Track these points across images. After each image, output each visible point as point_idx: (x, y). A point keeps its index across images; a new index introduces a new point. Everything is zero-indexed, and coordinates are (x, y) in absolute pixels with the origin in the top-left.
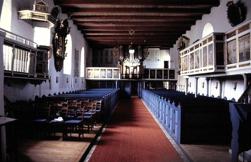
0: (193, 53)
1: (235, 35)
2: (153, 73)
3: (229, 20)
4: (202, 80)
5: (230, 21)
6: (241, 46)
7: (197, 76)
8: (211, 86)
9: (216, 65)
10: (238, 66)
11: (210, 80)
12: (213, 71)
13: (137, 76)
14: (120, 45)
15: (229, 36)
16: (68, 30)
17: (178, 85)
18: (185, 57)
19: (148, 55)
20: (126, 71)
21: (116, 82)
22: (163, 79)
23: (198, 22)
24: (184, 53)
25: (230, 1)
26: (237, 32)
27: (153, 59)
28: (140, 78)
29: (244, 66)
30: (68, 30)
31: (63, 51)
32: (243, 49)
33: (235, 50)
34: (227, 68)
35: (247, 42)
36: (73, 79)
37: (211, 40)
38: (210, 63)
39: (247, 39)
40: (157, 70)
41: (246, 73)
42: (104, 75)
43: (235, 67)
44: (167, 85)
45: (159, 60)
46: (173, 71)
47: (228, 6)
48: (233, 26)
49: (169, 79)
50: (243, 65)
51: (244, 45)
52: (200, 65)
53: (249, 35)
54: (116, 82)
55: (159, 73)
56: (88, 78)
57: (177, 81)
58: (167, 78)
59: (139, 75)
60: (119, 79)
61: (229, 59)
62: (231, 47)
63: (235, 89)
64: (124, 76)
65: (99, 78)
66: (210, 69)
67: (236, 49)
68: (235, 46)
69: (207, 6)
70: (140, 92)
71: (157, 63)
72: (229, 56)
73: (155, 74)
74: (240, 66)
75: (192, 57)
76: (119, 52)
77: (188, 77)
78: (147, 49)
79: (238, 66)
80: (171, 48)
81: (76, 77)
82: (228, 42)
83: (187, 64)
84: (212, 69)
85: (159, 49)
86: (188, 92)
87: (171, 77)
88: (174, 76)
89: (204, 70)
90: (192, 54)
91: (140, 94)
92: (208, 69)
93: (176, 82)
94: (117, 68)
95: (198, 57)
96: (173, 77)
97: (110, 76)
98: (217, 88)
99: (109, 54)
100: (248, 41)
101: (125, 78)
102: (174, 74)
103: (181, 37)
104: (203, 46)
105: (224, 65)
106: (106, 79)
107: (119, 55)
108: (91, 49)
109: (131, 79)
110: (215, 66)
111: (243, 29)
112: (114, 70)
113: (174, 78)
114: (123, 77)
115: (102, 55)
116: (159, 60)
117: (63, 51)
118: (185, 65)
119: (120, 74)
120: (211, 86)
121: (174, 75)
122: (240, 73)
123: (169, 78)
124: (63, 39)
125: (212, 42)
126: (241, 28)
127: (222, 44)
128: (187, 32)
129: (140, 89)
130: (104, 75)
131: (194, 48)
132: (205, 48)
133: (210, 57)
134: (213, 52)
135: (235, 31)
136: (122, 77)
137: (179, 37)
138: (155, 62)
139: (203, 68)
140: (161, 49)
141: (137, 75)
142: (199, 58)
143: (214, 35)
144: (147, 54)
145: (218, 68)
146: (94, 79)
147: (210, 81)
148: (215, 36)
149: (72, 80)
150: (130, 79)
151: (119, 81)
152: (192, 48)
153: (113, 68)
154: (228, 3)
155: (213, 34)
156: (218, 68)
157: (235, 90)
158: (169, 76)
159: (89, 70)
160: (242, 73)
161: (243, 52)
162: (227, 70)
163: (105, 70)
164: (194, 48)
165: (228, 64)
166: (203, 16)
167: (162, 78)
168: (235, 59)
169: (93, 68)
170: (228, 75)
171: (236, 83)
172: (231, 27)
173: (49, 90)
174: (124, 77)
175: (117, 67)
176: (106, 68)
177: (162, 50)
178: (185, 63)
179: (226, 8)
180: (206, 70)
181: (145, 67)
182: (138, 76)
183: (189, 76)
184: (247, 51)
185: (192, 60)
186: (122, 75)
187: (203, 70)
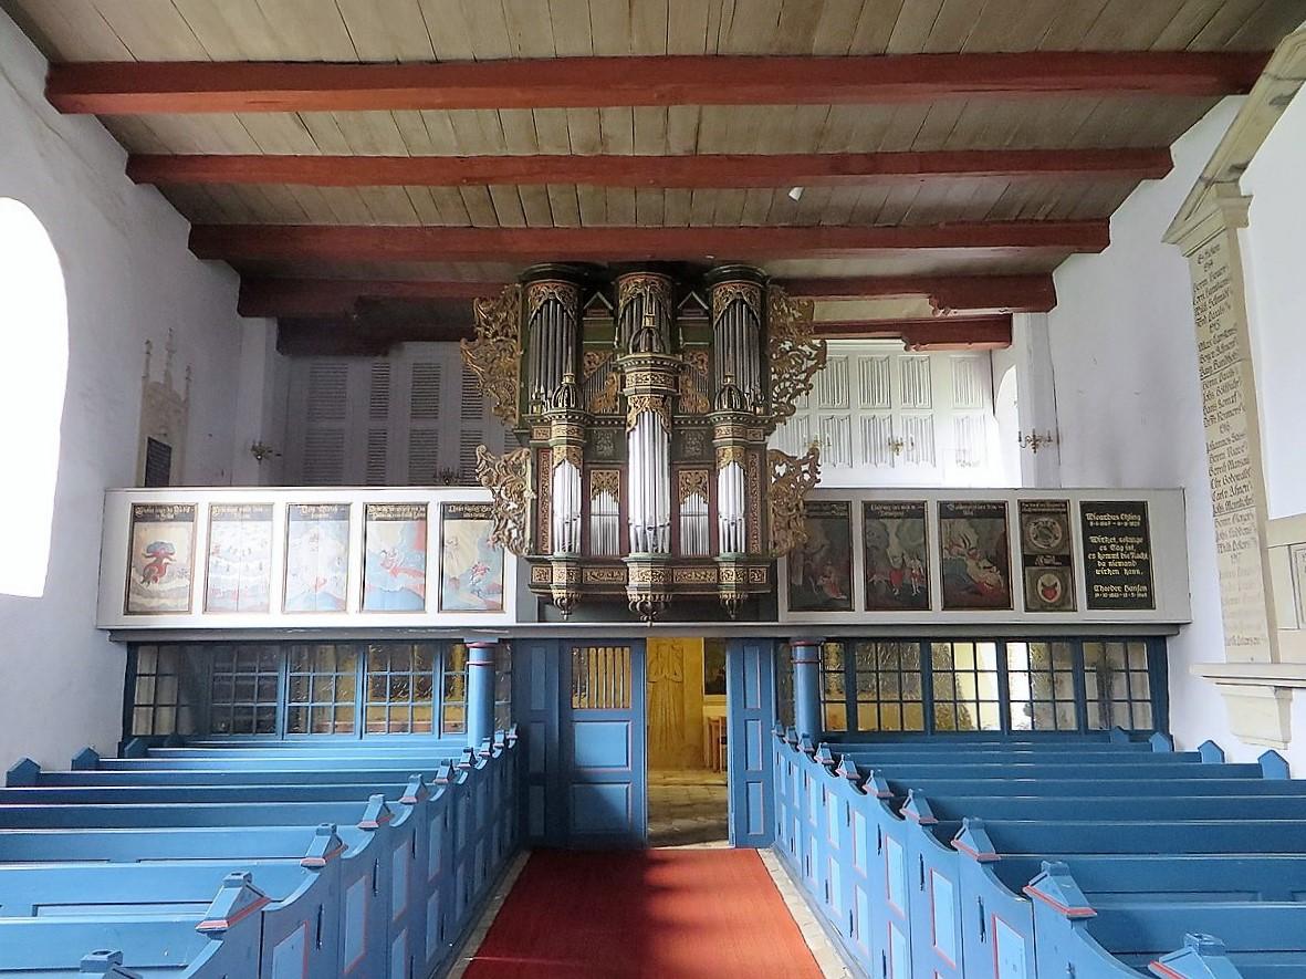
2: (894, 549)
13: (717, 586)
19: (810, 371)
21: (475, 656)
28: (757, 604)
40: (949, 511)
46: (1132, 520)
54: (475, 656)
55: (973, 538)
56: (128, 612)
58: (1066, 603)
60: (508, 618)
64: (560, 575)
65: (267, 610)
70: (756, 763)
73: (925, 561)
80: (1021, 321)
85: (899, 344)
87: (1106, 580)
88: (1146, 579)
91: (756, 791)
94: (482, 495)
96: (1136, 584)
97: (403, 581)
99: (450, 395)
101: (570, 606)
107: (524, 378)
113: (1148, 603)
115: (379, 403)
116: (896, 446)
119: (511, 560)
121: (1145, 566)
123: (1093, 604)
129: (755, 729)
138: (858, 458)
141: (710, 562)
146: (198, 620)
153: (434, 497)
158: (1091, 580)
159: (143, 514)
163: (343, 512)
167: (1006, 604)
174: (556, 594)
176: (357, 497)
181: (814, 470)
182: (730, 576)
186: (536, 574)
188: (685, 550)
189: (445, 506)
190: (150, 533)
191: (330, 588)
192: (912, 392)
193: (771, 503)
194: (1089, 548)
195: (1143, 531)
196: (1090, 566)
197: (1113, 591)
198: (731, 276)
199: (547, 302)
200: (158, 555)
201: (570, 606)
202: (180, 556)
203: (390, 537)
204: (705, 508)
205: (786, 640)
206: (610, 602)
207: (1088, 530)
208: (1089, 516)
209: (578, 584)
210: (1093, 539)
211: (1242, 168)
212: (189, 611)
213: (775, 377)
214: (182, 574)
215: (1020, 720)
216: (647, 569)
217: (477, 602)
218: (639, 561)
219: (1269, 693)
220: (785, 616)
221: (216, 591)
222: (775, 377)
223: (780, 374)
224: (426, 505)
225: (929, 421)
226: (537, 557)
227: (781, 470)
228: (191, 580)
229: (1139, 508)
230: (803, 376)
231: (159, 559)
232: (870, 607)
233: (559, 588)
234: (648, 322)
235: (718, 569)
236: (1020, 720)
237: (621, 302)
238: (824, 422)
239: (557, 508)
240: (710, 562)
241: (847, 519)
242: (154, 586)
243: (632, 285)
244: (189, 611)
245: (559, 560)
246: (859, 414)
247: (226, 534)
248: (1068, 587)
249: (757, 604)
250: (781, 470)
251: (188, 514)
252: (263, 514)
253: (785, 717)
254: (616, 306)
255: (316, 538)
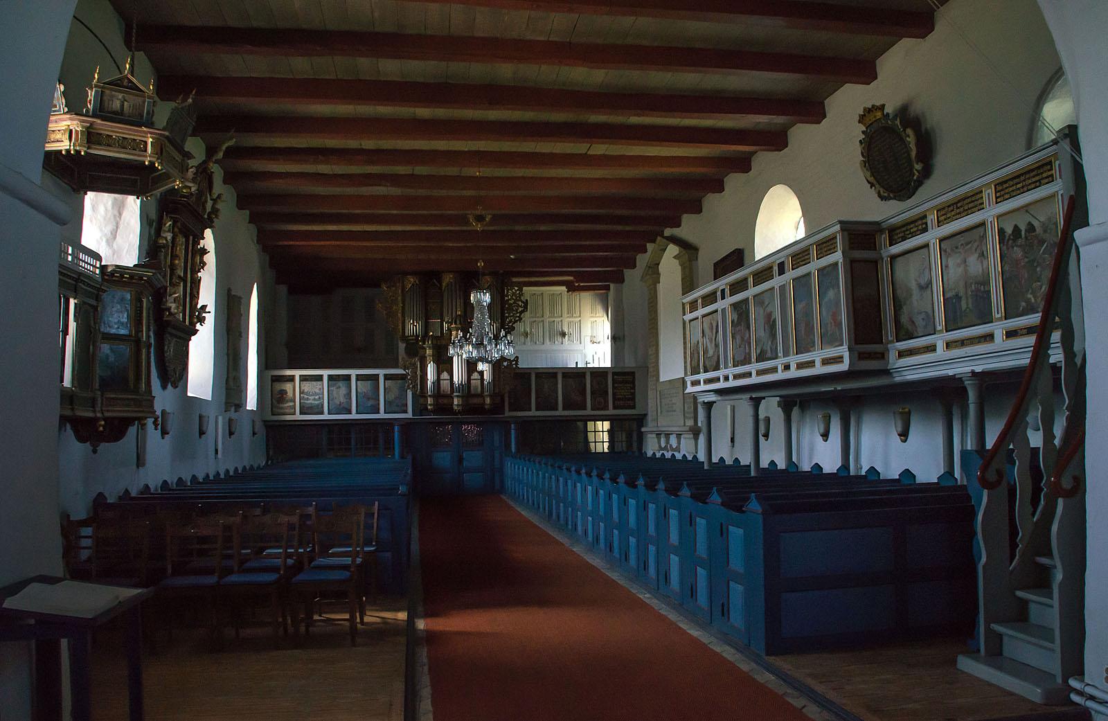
0: (746, 301)
1: (925, 230)
3: (869, 174)
4: (771, 407)
5: (871, 179)
6: (951, 271)
7: (755, 393)
8: (798, 432)
9: (856, 343)
10: (940, 346)
11: (795, 405)
12: (844, 366)
13: (484, 403)
14: (406, 274)
15: (898, 232)
16: (209, 209)
17: (652, 432)
18: (704, 316)
20: (439, 379)
22: (589, 412)
23: (734, 181)
24: (700, 301)
25: (873, 106)
26: (932, 218)
27: (541, 330)
28: (497, 408)
29: (967, 345)
30: (209, 204)
31: (188, 300)
32: (962, 284)
33: (927, 286)
34: (893, 355)
35: (977, 255)
36: (220, 419)
37: (832, 250)
38: (830, 339)
39: (976, 244)
41: (978, 369)
42: (342, 400)
43: (931, 348)
44: (600, 434)
45: (563, 334)
46: (629, 378)
47: (865, 125)
48: (882, 198)
49: (611, 411)
50: (963, 343)
51: (963, 266)
52: (780, 348)
53: (981, 230)
56: (273, 414)
57: (646, 415)
58: (606, 408)
59: (490, 396)
60: (409, 415)
61: (904, 319)
62: (908, 273)
63: (904, 435)
64: (430, 401)
65: (322, 413)
66: (826, 362)
67: (930, 282)
68: (927, 271)
69: (779, 120)
71: (555, 347)
72: (901, 307)
74: (949, 345)
75: (740, 315)
76: (403, 302)
77: (712, 397)
78: (521, 290)
79: (940, 346)
81: (232, 414)
82: (893, 258)
83: (717, 346)
84: (839, 360)
85: (564, 288)
86: (715, 460)
87: (619, 399)
88: (633, 399)
89: (800, 366)
90: (740, 309)
92: (818, 363)
93: (641, 420)
95: (769, 315)
96: (630, 401)
97: (371, 403)
98: (825, 436)
100: (978, 251)
101: (434, 412)
102: (634, 388)
103: (659, 238)
104: (790, 274)
105: (882, 343)
106: (354, 416)
107: (403, 316)
108: (283, 290)
109: (459, 412)
110: (850, 349)
111: (958, 208)
112: (387, 377)
114: (426, 405)
116: (563, 334)
117: (188, 300)
118: (705, 352)
119: (410, 393)
120: (798, 432)
121: (633, 394)
122: (951, 373)
123: (615, 408)
124: (187, 241)
125: (837, 256)
126: (949, 206)
127: (875, 263)
128: (686, 219)
130: (342, 400)
131: (751, 280)
132: (802, 283)
133: (824, 313)
134: (841, 292)
135: (925, 217)
136: (420, 409)
137: (654, 241)
139: (793, 360)
140: (571, 288)
141: (481, 395)
142: (774, 321)
143: (842, 230)
144: (520, 309)
145: (863, 356)
147: (795, 412)
148: (846, 233)
149: (217, 425)
150: (455, 413)
151: (406, 425)
152: (742, 281)
153: (381, 372)
154: (869, 111)
155: (838, 227)
156: (863, 356)
157: (905, 441)
158: (614, 399)
160: (961, 369)
161: (961, 294)
162: (894, 362)
163: (348, 378)
164: (751, 280)
165: (897, 341)
166: (753, 159)
168: (930, 319)
169: (297, 373)
170: (898, 379)
171: (909, 413)
172: (879, 200)
173: (135, 467)
174: (429, 407)
175: (396, 366)
176: (353, 373)
177: (576, 293)
178: (706, 340)
179: (858, 131)
180: (811, 364)
181: (517, 364)
182: (488, 401)
183: (719, 392)
184: (977, 290)
185: (742, 327)
186: (422, 400)
187: (793, 366)
188: (473, 392)
189: (385, 375)
190: (279, 386)
191: (346, 406)
192: (571, 312)
193: (502, 376)
194: (614, 388)
195: (633, 382)
196: (614, 394)
197: (621, 403)
198: (489, 274)
199: (413, 285)
200: (283, 392)
201: (434, 412)
202: (290, 394)
203: (365, 387)
204: (479, 377)
205: (509, 421)
206: (447, 409)
207: (614, 381)
208: (615, 377)
209: (435, 405)
210: (616, 385)
211: (659, 264)
212: (295, 414)
213: (507, 315)
214: (291, 401)
215: (606, 450)
216: (460, 399)
217: (397, 409)
218: (457, 396)
219: (654, 436)
220: (507, 414)
221: (304, 407)
222: (507, 315)
223: (509, 313)
224: (378, 375)
225: (579, 323)
226: (421, 395)
227: (505, 364)
228: (295, 402)
229: (633, 374)
230: (518, 315)
231: (282, 395)
232: (537, 409)
233: (430, 405)
234: (459, 313)
235: (484, 398)
236: (606, 450)
237: (444, 284)
238: (532, 323)
239: (429, 377)
240: (481, 395)
241: (529, 379)
242: (281, 405)
243: (448, 279)
244: (295, 414)
245: (429, 396)
246: (547, 320)
247: (307, 386)
248: (606, 402)
249: (497, 408)
250: (505, 364)
251: (292, 379)
252: (319, 378)
253: (508, 446)
254: (441, 285)
255: (339, 387)
